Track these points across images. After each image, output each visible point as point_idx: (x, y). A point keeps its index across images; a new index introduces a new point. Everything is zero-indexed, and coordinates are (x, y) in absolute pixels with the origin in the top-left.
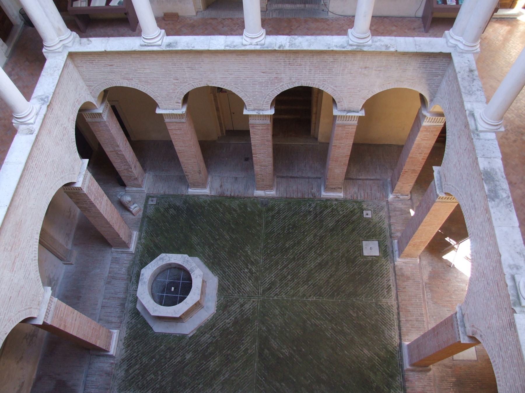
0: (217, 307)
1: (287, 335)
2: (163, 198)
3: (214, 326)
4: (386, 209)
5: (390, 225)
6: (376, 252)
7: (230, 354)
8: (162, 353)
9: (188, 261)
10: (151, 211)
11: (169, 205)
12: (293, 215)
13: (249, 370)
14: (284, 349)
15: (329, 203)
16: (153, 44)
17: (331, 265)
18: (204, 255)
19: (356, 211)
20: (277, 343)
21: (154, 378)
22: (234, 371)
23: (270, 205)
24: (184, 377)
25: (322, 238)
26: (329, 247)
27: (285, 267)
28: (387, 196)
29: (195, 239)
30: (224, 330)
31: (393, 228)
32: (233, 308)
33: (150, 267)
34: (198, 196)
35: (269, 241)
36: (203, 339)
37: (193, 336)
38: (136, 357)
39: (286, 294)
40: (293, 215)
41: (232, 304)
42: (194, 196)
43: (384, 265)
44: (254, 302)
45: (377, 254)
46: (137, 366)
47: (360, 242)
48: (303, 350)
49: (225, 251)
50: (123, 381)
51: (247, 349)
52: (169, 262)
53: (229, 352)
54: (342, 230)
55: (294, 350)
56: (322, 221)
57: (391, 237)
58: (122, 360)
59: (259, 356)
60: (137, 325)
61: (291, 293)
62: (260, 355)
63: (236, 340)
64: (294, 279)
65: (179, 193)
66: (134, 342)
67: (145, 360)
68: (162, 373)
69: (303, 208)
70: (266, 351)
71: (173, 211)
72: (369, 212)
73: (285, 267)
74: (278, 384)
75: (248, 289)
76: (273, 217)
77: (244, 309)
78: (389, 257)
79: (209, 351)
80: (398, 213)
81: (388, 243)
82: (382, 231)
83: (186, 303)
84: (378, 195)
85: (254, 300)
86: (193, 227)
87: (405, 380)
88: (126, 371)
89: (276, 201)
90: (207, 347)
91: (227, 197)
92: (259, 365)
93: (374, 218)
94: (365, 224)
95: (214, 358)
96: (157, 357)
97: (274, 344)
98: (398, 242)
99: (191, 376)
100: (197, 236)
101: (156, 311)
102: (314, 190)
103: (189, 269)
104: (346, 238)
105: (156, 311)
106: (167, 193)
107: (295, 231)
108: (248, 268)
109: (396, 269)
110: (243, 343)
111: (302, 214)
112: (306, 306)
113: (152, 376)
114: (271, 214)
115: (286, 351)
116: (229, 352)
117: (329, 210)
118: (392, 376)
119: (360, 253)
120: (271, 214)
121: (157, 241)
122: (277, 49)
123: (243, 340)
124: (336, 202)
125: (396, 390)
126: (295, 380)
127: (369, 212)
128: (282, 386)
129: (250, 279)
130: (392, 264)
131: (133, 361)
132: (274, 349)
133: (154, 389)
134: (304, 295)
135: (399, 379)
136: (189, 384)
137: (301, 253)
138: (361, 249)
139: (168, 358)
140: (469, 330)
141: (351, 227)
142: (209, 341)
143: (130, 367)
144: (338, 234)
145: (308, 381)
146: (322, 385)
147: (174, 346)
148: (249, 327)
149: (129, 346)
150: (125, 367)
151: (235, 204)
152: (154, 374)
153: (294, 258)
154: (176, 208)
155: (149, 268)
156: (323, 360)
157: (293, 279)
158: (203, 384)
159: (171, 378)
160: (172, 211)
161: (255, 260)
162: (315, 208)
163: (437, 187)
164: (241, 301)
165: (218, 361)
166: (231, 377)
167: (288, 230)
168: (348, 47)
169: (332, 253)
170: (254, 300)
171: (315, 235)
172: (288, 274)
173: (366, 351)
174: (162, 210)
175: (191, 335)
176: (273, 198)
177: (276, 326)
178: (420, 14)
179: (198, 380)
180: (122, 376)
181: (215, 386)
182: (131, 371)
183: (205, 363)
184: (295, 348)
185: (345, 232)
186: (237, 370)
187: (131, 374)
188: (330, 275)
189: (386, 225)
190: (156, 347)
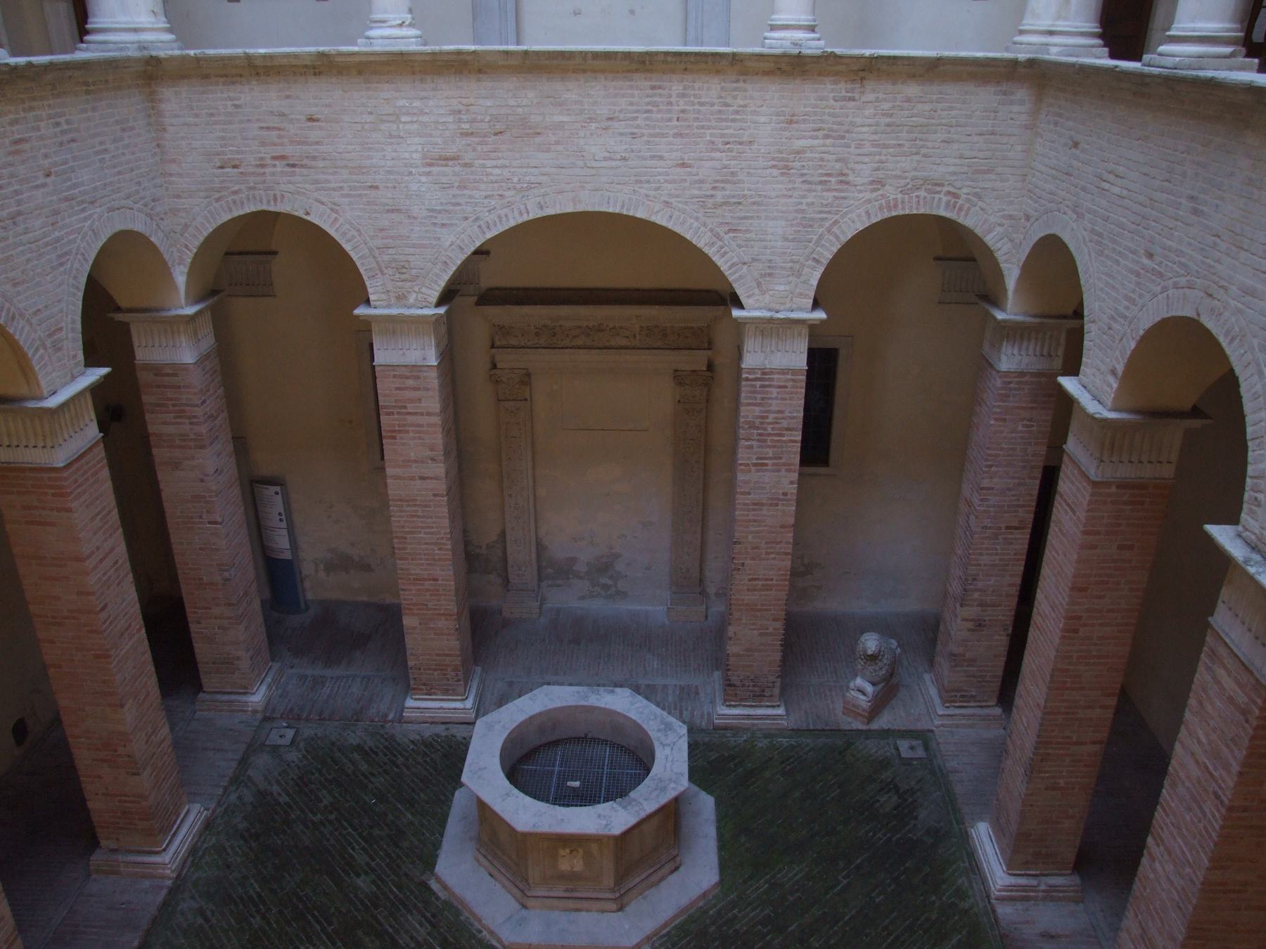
8: (390, 817)
9: (664, 789)
10: (873, 748)
33: (638, 705)
37: (430, 889)
42: (972, 855)
46: (364, 767)
52: (656, 744)
58: (392, 736)
68: (330, 822)
79: (367, 939)
83: (508, 795)
86: (841, 864)
88: (358, 746)
121: (767, 774)
133: (290, 807)
147: (406, 844)
155: (632, 704)
160: (888, 802)
175: (434, 885)
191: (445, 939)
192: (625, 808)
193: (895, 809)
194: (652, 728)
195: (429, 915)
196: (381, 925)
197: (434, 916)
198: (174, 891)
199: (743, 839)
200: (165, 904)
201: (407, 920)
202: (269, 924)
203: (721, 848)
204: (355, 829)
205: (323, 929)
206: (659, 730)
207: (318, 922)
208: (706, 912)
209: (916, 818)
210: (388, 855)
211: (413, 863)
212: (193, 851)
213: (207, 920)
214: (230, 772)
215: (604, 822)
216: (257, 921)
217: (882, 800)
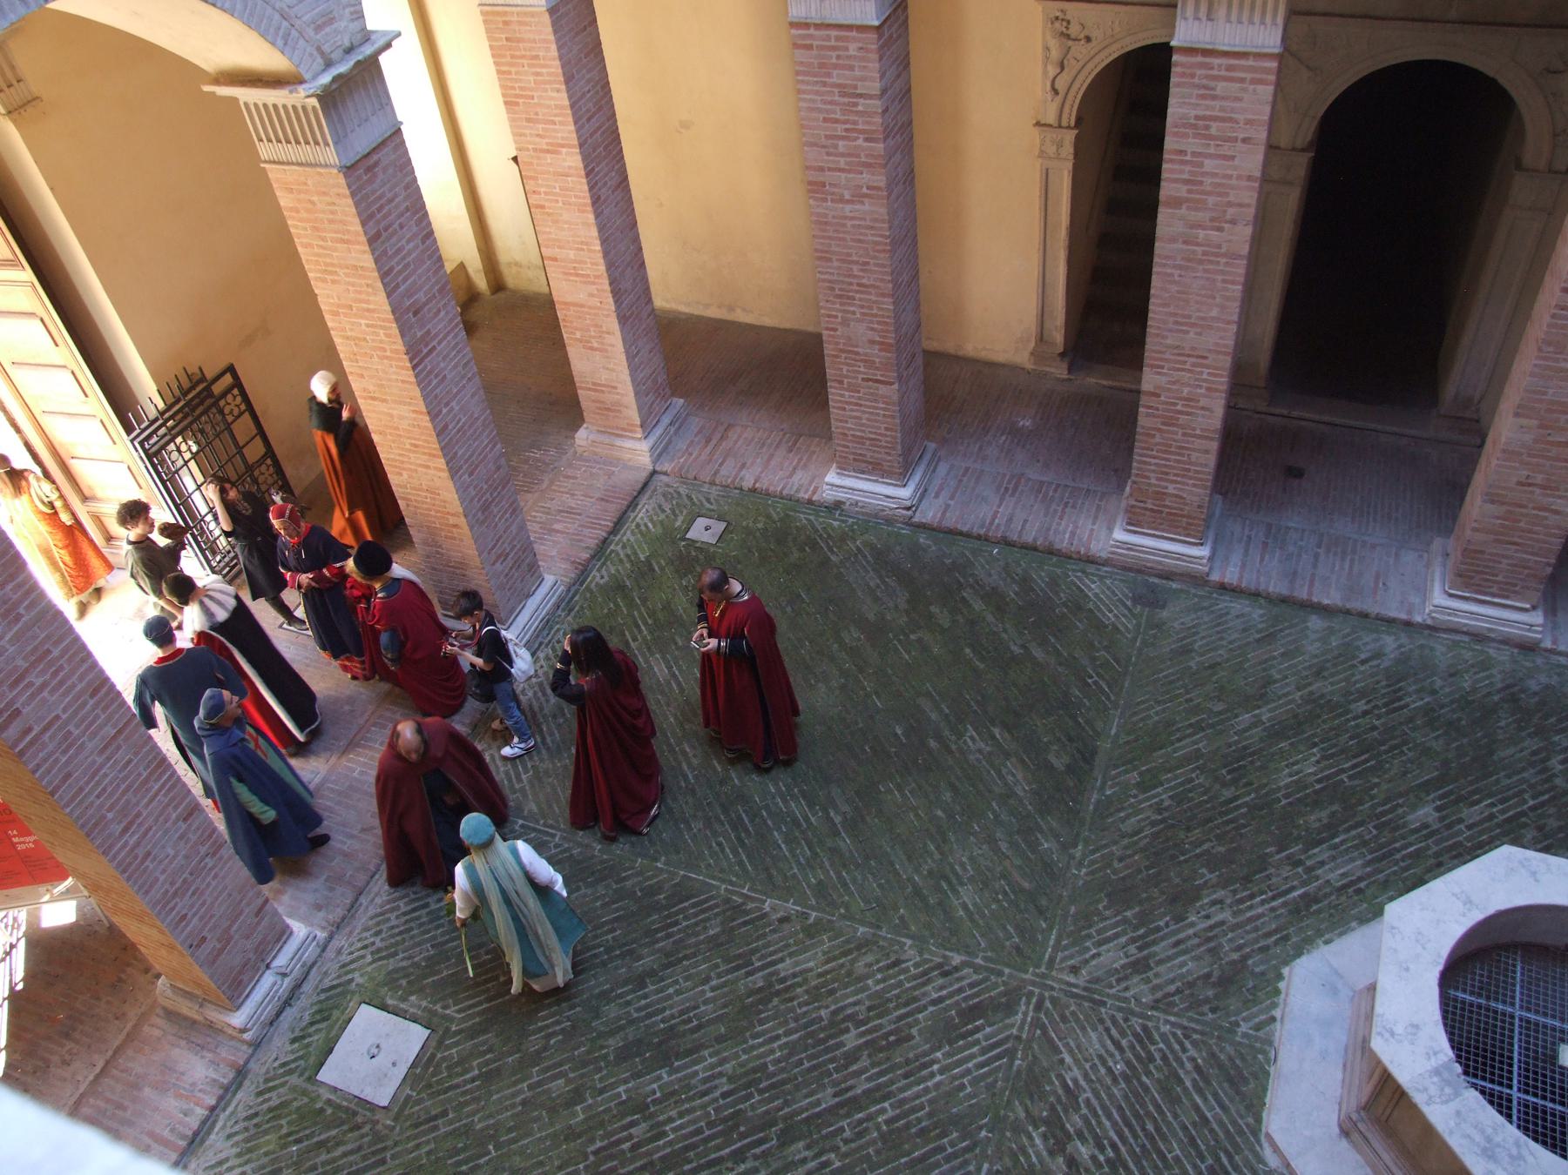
0: (1277, 992)
1: (947, 796)
3: (1300, 909)
6: (367, 1022)
7: (1224, 785)
13: (1149, 717)
14: (980, 751)
17: (612, 1033)
20: (1001, 777)
22: (1212, 726)
24: (1437, 746)
26: (571, 1135)
27: (855, 1104)
30: (1247, 880)
31: (194, 1122)
32: (1191, 967)
39: (896, 963)
41: (1191, 985)
43: (379, 950)
44: (1074, 970)
47: (400, 1105)
51: (1143, 787)
53: (1227, 793)
55: (939, 737)
57: (241, 1073)
59: (1094, 753)
61: (870, 958)
62: (1087, 756)
63: (1188, 829)
64: (832, 1024)
68: (1549, 779)
70: (1059, 762)
73: (855, 1104)
74: (1038, 653)
75: (1094, 1041)
77: (1132, 949)
78: (327, 983)
79: (1324, 814)
81: (280, 1047)
82: (256, 1125)
83: (1468, 902)
85: (1072, 979)
87: (584, 571)
90: (1331, 828)
92: (1099, 725)
95: (1300, 785)
97: (1018, 778)
99: (1405, 743)
104: (457, 1152)
108: (1072, 1162)
109: (340, 912)
110: (1159, 811)
112: (820, 882)
116: (1227, 793)
119: (440, 1042)
123: (1153, 824)
125: (628, 556)
126: (967, 651)
128: (1023, 646)
129: (1072, 1094)
132: (1023, 761)
134: (812, 931)
135: (598, 577)
136: (1411, 720)
137: (739, 1156)
138: (422, 1071)
139: (1525, 825)
142: (1321, 852)
145: (920, 640)
146: (871, 616)
148: (1116, 865)
153: (787, 1138)
156: (834, 684)
157: (838, 1025)
158: (1348, 712)
164: (1137, 988)
166: (1226, 711)
169: (577, 1096)
170: (1072, 979)
172: (852, 1057)
177: (992, 841)
183: (1344, 777)
184: (933, 744)
188: (643, 985)
191: (1317, 901)
192: (1437, 1072)
195: (1362, 885)
196: (1348, 830)
197: (1359, 891)
200: (1391, 621)
201: (1353, 860)
202: (1354, 718)
204: (1531, 809)
205: (1343, 771)
207: (1354, 766)
212: (1478, 637)
213: (1363, 662)
215: (1399, 1029)
216: (1361, 706)
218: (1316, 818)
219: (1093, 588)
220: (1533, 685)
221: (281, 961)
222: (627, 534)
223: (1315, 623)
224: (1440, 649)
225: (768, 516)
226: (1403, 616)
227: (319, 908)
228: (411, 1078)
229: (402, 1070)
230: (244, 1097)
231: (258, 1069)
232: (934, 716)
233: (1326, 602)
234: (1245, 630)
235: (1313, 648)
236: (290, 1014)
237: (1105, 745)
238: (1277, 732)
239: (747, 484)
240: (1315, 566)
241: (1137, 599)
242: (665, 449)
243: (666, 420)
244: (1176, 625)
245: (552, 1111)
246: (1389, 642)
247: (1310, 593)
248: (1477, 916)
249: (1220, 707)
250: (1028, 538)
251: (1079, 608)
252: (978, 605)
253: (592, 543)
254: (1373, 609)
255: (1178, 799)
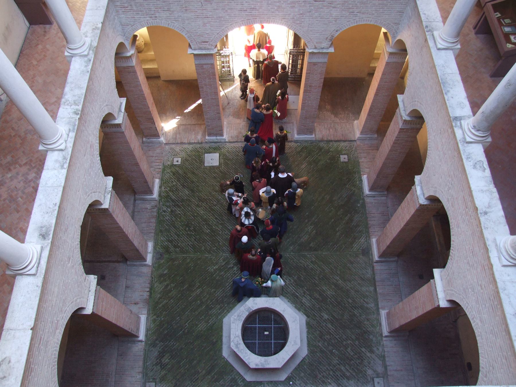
2: (147, 374)
3: (294, 295)
4: (173, 146)
5: (190, 143)
9: (238, 316)
11: (157, 364)
12: (175, 227)
15: (163, 194)
16: (39, 257)
18: (219, 314)
19: (174, 170)
21: (350, 348)
23: (161, 251)
25: (201, 200)
28: (160, 143)
29: (202, 327)
31: (192, 141)
33: (247, 358)
34: (147, 330)
35: (203, 248)
36: (308, 304)
38: (334, 372)
40: (175, 227)
45: (217, 155)
46: (343, 368)
47: (206, 168)
48: (307, 214)
49: (215, 292)
50: (358, 380)
51: (312, 262)
53: (316, 278)
54: (193, 183)
55: (309, 221)
56: (183, 200)
57: (202, 143)
60: (302, 377)
65: (142, 353)
66: (320, 376)
67: (335, 361)
69: (167, 218)
70: (311, 245)
71: (165, 357)
72: (175, 159)
74: (338, 234)
76: (175, 247)
79: (318, 297)
80: (178, 136)
81: (207, 146)
82: (196, 150)
84: (158, 151)
86: (186, 331)
87: (322, 141)
88: (349, 380)
89: (158, 245)
90: (315, 299)
91: (150, 296)
93: (181, 156)
94: (187, 163)
95: (324, 291)
96: (331, 348)
98: (210, 135)
100: (197, 325)
101: (295, 342)
102: (149, 206)
103: (247, 313)
105: (295, 342)
106: (141, 369)
107: (192, 224)
108: (233, 267)
111: (174, 219)
113: (349, 350)
114: (172, 249)
115: (310, 228)
117: (171, 194)
118: (320, 149)
120: (172, 249)
121: (204, 372)
122: (79, 116)
123: (304, 266)
124: (163, 187)
127: (175, 159)
128: (339, 230)
130: (227, 144)
131: (338, 373)
135: (322, 144)
136: (351, 312)
137: (216, 218)
138: (212, 168)
140: (326, 44)
141: (190, 175)
143: (344, 376)
144: (198, 186)
146: (334, 199)
147: (318, 332)
149: (324, 382)
150: (345, 381)
151: (159, 287)
152: (347, 349)
154: (161, 355)
155: (249, 358)
159: (348, 330)
160: (166, 360)
161: (224, 260)
162: (167, 207)
163: (208, 53)
165: (326, 287)
167: (191, 231)
168: (89, 57)
171: (198, 206)
173: (303, 166)
174: (163, 372)
176: (155, 248)
178: (28, 24)
179: (345, 304)
180: (354, 383)
181: (348, 287)
182: (348, 374)
184: (306, 221)
185: (195, 180)
186: (331, 269)
187: (351, 373)
189: (190, 147)
190: (322, 351)
192: (249, 308)
193: (164, 356)
194: (242, 346)
198: (378, 309)
199: (215, 340)
200: (378, 305)
203: (222, 336)
206: (240, 344)
208: (227, 311)
209: (159, 352)
210: (322, 327)
211: (313, 325)
212: (380, 324)
214: (387, 359)
216: (350, 301)
217: (167, 360)
218: (317, 295)
219: (362, 240)
220: (371, 337)
221: (218, 138)
222: (335, 144)
223: (372, 289)
224: (375, 316)
225: (353, 169)
226: (380, 307)
227: (231, 137)
228: (210, 167)
229: (211, 165)
230: (199, 145)
231: (203, 145)
232: (313, 219)
233: (377, 289)
234: (363, 274)
235: (364, 289)
236: (213, 144)
237: (320, 252)
238: (336, 285)
239: (360, 160)
240: (388, 285)
241: (363, 250)
242: (362, 140)
243: (368, 136)
244: (359, 259)
245: (213, 189)
246: (372, 305)
247: (378, 286)
248: (282, 313)
249: (339, 272)
250: (369, 222)
251: (355, 239)
252: (347, 218)
253: (329, 139)
254: (379, 300)
255: (312, 269)
